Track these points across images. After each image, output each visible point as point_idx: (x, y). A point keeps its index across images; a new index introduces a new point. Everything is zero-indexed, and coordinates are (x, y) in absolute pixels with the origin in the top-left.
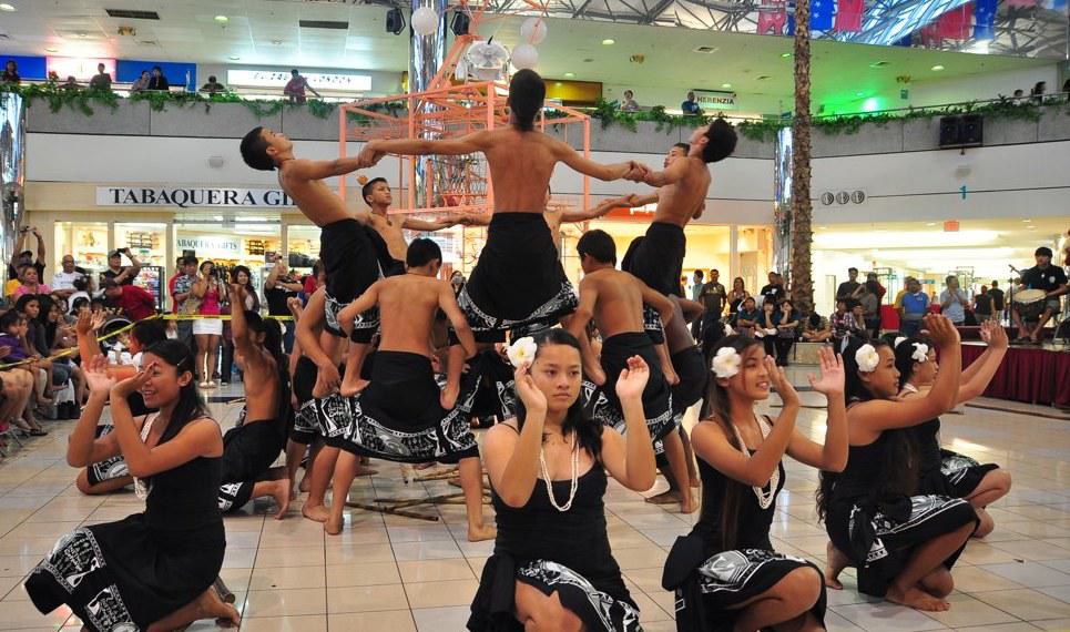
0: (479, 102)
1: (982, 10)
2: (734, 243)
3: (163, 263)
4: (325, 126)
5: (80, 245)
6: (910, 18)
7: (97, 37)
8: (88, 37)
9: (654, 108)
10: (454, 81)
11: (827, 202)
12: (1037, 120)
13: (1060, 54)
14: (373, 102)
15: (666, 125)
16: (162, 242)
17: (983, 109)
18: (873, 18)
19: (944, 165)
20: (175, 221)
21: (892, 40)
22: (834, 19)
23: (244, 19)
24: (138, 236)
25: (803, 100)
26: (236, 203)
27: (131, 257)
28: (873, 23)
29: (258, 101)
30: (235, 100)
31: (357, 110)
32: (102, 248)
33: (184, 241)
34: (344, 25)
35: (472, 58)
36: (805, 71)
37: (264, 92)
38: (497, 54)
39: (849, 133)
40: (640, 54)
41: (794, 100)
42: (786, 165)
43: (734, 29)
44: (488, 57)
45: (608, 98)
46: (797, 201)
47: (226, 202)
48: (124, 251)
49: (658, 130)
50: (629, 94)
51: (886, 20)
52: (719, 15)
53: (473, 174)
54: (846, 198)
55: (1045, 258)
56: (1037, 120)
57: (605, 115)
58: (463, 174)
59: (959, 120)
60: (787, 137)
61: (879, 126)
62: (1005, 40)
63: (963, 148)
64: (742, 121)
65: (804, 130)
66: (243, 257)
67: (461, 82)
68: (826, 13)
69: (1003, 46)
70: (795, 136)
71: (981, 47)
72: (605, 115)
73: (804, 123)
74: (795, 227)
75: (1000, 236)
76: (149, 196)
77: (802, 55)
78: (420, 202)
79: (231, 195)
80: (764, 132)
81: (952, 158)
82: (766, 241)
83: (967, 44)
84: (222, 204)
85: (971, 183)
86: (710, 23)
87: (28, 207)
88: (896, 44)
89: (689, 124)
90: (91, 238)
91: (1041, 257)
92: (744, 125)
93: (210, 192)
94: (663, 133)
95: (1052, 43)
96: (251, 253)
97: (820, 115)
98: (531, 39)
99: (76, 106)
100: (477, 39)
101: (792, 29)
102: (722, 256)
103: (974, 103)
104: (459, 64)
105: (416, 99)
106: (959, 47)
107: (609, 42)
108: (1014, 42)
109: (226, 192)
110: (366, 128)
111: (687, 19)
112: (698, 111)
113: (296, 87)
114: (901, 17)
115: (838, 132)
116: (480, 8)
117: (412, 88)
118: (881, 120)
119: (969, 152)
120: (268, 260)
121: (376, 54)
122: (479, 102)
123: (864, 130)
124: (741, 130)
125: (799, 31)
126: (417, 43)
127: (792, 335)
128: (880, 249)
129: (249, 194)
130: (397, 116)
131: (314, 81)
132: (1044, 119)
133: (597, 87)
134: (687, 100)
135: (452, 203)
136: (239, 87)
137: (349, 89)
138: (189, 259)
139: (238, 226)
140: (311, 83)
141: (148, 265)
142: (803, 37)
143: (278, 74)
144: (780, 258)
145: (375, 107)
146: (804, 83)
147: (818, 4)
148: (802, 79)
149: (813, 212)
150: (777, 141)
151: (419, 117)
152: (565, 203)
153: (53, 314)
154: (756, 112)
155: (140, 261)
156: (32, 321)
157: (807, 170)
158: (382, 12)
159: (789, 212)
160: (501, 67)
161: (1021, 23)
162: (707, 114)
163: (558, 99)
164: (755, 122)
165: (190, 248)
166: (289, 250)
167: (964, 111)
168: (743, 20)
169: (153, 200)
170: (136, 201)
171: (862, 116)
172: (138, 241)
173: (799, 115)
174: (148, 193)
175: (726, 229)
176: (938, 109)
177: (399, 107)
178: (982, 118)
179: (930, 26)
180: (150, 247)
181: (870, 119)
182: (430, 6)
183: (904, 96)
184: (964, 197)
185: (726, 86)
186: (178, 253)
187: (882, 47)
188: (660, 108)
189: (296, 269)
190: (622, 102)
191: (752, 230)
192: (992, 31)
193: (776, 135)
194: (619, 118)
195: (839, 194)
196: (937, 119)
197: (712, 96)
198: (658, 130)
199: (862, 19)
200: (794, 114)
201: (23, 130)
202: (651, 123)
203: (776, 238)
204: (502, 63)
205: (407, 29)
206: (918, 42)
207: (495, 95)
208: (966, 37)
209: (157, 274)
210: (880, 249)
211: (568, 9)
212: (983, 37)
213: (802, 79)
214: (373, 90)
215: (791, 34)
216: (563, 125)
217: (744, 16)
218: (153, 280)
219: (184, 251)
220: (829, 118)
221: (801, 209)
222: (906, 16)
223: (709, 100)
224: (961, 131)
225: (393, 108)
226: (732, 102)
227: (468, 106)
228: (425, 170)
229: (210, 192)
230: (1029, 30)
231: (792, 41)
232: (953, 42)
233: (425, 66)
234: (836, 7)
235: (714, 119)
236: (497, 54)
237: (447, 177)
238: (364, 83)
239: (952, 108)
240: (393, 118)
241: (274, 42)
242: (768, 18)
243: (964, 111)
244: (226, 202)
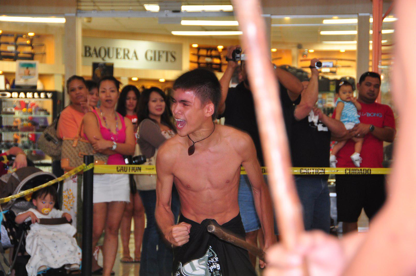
24: (11, 40)
141: (33, 89)
180: (32, 56)
209: (48, 105)
218: (42, 114)
219: (95, 65)
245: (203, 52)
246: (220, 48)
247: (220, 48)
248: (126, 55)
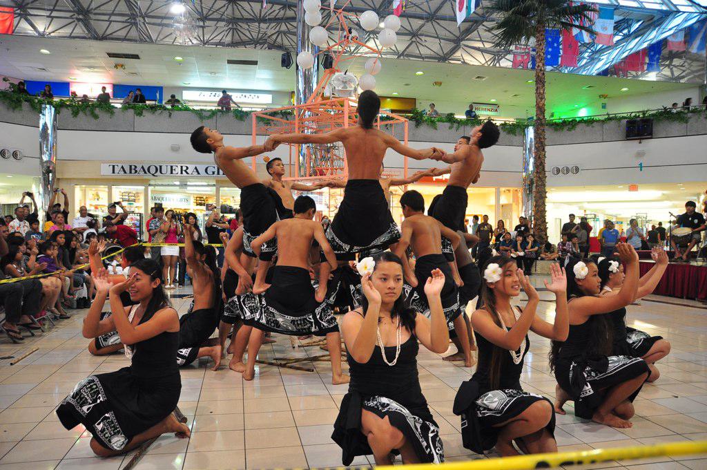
0: (339, 111)
1: (652, 53)
2: (498, 199)
3: (142, 211)
4: (243, 125)
5: (91, 200)
6: (608, 58)
7: (101, 70)
8: (96, 70)
9: (448, 115)
10: (324, 98)
12: (687, 122)
13: (700, 81)
14: (275, 110)
15: (455, 125)
16: (142, 198)
17: (653, 115)
18: (584, 58)
19: (628, 150)
20: (150, 185)
21: (596, 72)
22: (560, 59)
23: (193, 59)
25: (541, 109)
26: (187, 173)
27: (122, 207)
28: (584, 61)
29: (201, 110)
30: (187, 109)
31: (262, 115)
32: (104, 202)
33: (155, 197)
34: (255, 63)
35: (335, 83)
36: (542, 91)
37: (205, 104)
38: (350, 81)
40: (436, 81)
41: (535, 109)
42: (530, 150)
43: (498, 65)
44: (345, 83)
45: (419, 108)
46: (537, 172)
47: (182, 173)
48: (118, 203)
49: (450, 128)
50: (433, 106)
51: (592, 60)
52: (488, 57)
53: (335, 155)
55: (691, 208)
56: (687, 122)
57: (418, 119)
60: (531, 133)
62: (666, 72)
64: (503, 122)
66: (192, 207)
67: (328, 98)
68: (555, 55)
69: (665, 75)
70: (536, 132)
71: (652, 76)
72: (418, 119)
73: (541, 124)
74: (536, 188)
75: (663, 194)
76: (133, 169)
77: (540, 81)
78: (302, 173)
79: (184, 168)
80: (516, 129)
81: (634, 146)
82: (518, 198)
83: (642, 75)
84: (179, 174)
85: (645, 161)
86: (483, 61)
87: (58, 176)
88: (599, 74)
90: (97, 195)
91: (689, 207)
92: (504, 125)
93: (172, 167)
94: (454, 129)
95: (696, 74)
96: (197, 205)
98: (372, 72)
99: (88, 113)
100: (338, 71)
101: (534, 64)
102: (490, 206)
104: (326, 87)
105: (300, 109)
106: (638, 76)
107: (420, 73)
108: (672, 73)
109: (182, 167)
110: (269, 127)
111: (468, 59)
112: (476, 116)
113: (225, 101)
114: (602, 58)
116: (340, 52)
117: (298, 103)
118: (589, 122)
119: (644, 142)
120: (207, 209)
121: (275, 80)
122: (339, 111)
123: (579, 128)
125: (539, 66)
126: (300, 74)
127: (534, 256)
128: (588, 202)
129: (196, 168)
130: (288, 120)
131: (236, 97)
132: (691, 121)
133: (413, 101)
134: (468, 109)
135: (322, 174)
136: (189, 101)
137: (259, 102)
138: (158, 208)
139: (189, 188)
140: (234, 98)
141: (133, 212)
142: (541, 70)
143: (214, 93)
144: (526, 208)
145: (274, 114)
146: (542, 99)
147: (550, 50)
148: (540, 96)
150: (524, 135)
151: (302, 120)
152: (393, 173)
153: (73, 243)
154: (511, 117)
155: (128, 210)
156: (61, 247)
158: (279, 54)
159: (532, 179)
160: (353, 89)
161: (676, 62)
162: (480, 118)
163: (388, 108)
164: (511, 123)
165: (160, 202)
166: (221, 203)
168: (503, 59)
169: (136, 172)
170: (125, 172)
171: (578, 119)
172: (127, 197)
173: (539, 119)
174: (133, 167)
175: (493, 190)
176: (625, 115)
177: (289, 113)
178: (653, 120)
179: (620, 63)
181: (582, 121)
182: (308, 51)
183: (604, 107)
184: (641, 170)
185: (493, 101)
186: (151, 205)
187: (592, 76)
188: (452, 114)
189: (225, 215)
190: (428, 110)
191: (509, 191)
192: (658, 67)
193: (524, 131)
196: (624, 121)
197: (484, 107)
198: (450, 128)
199: (578, 59)
200: (535, 118)
201: (55, 128)
202: (445, 123)
204: (353, 86)
205: (294, 65)
206: (613, 74)
207: (349, 106)
208: (643, 70)
209: (138, 218)
210: (588, 202)
211: (394, 53)
212: (653, 70)
213: (540, 96)
214: (273, 103)
215: (533, 68)
216: (391, 125)
217: (504, 57)
218: (136, 222)
219: (156, 204)
220: (557, 121)
222: (604, 57)
223: (482, 109)
224: (639, 129)
225: (286, 114)
226: (496, 110)
227: (332, 113)
228: (306, 153)
229: (172, 167)
230: (682, 66)
231: (534, 73)
232: (634, 73)
233: (305, 90)
234: (561, 51)
235: (485, 121)
236: (350, 81)
238: (267, 99)
239: (633, 114)
240: (285, 121)
241: (211, 73)
242: (519, 58)
244: (182, 173)
245: (198, 199)
246: (205, 197)
247: (205, 197)
248: (170, 200)
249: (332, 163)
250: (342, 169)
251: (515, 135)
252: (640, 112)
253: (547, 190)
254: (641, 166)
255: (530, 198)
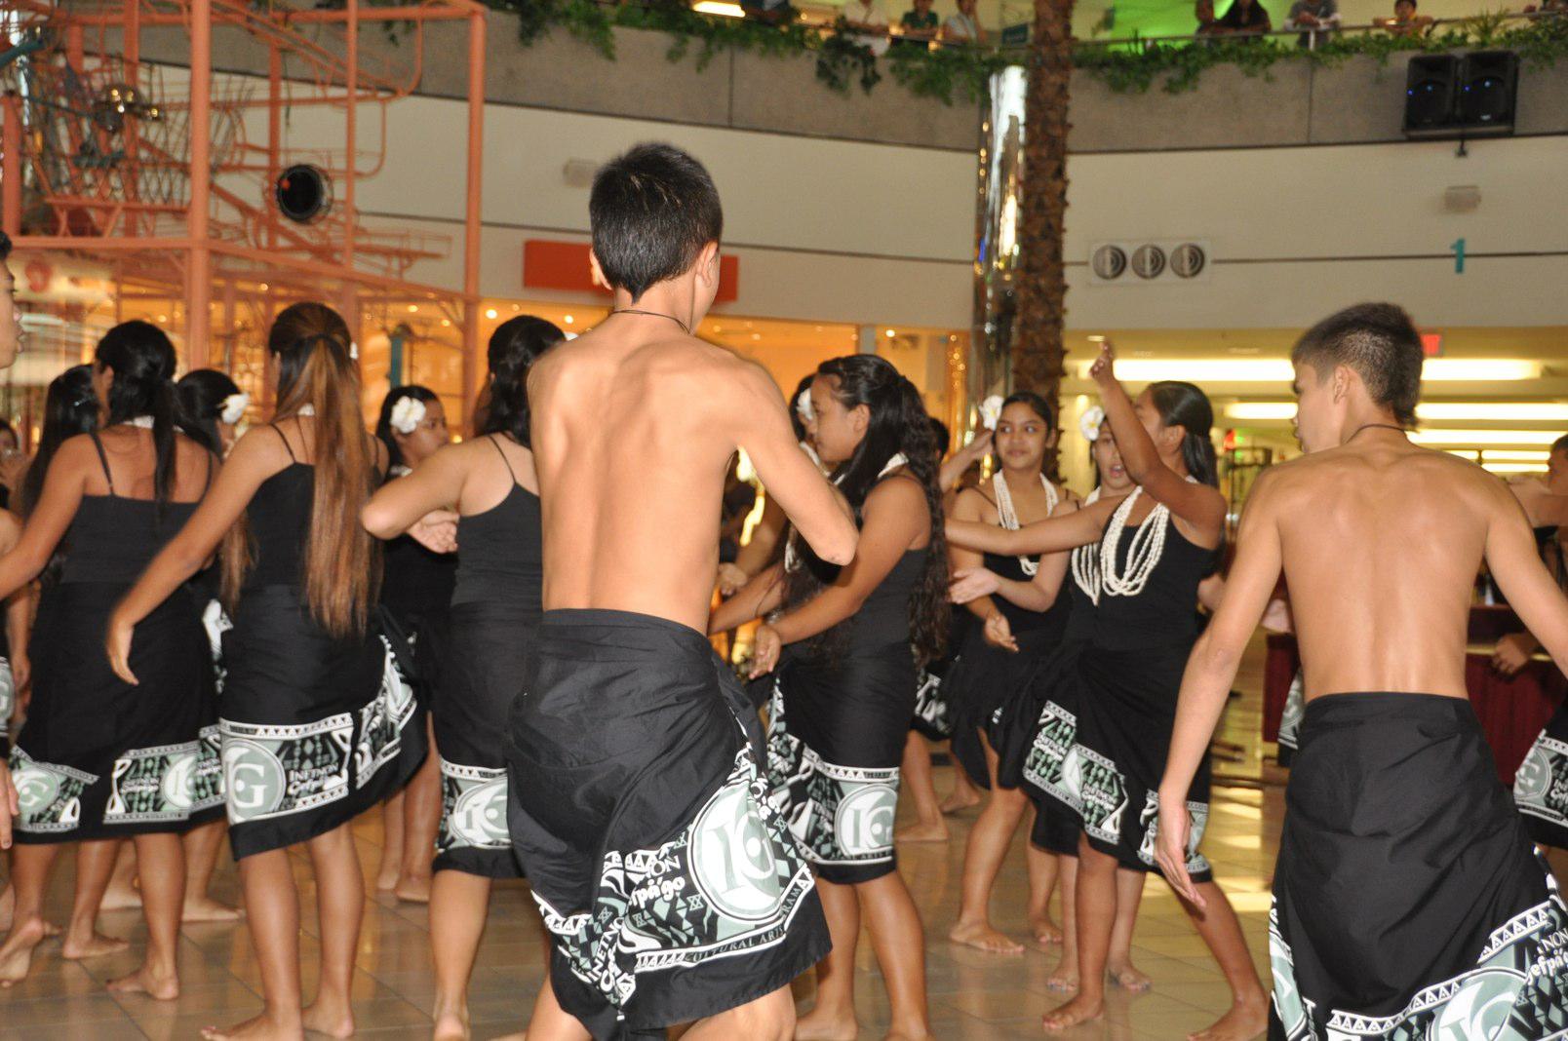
11: (1108, 269)
15: (695, 44)
39: (1172, 88)
49: (674, 56)
53: (150, 147)
54: (1158, 262)
58: (116, 143)
59: (1458, 62)
60: (1011, 92)
61: (1250, 74)
63: (1463, 138)
65: (1054, 79)
70: (1032, 99)
81: (1434, 164)
82: (950, 369)
89: (758, 46)
94: (688, 63)
97: (1104, 35)
103: (1497, 19)
115: (1145, 86)
124: (893, 69)
135: (81, 225)
149: (1070, 300)
150: (985, 105)
157: (1059, 184)
167: (1472, 39)
173: (1043, 39)
178: (1516, 59)
184: (1460, 269)
191: (913, 340)
193: (985, 88)
194: (567, 15)
195: (1141, 250)
196: (1400, 61)
198: (674, 56)
203: (974, 357)
216: (410, 24)
220: (1124, 48)
221: (1038, 290)
235: (824, 35)
237: (66, 146)
239: (1440, 31)
243: (1472, 39)
249: (135, 183)
250: (180, 213)
251: (949, 103)
252: (1473, 20)
253: (1067, 345)
254: (1460, 256)
255: (999, 370)
